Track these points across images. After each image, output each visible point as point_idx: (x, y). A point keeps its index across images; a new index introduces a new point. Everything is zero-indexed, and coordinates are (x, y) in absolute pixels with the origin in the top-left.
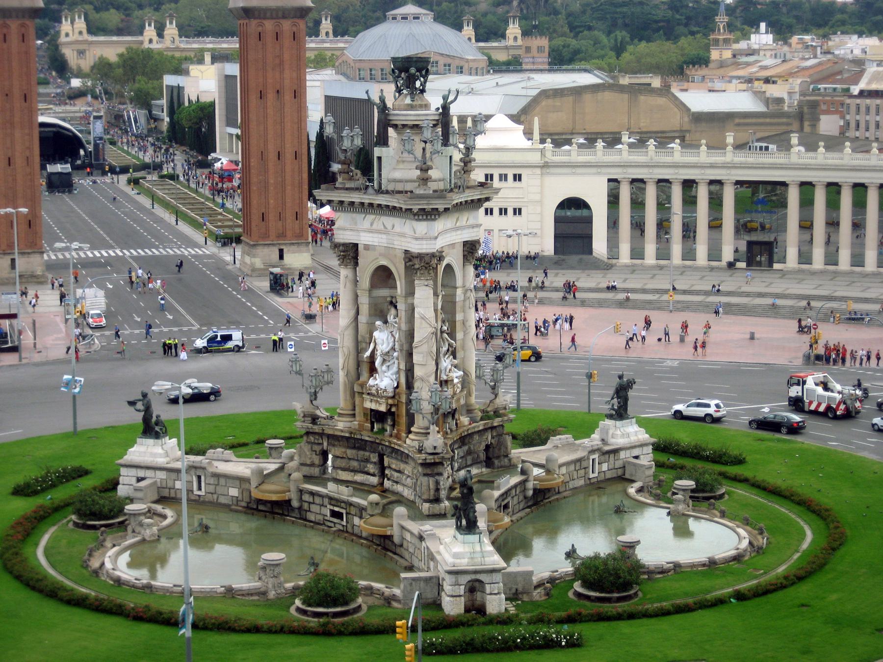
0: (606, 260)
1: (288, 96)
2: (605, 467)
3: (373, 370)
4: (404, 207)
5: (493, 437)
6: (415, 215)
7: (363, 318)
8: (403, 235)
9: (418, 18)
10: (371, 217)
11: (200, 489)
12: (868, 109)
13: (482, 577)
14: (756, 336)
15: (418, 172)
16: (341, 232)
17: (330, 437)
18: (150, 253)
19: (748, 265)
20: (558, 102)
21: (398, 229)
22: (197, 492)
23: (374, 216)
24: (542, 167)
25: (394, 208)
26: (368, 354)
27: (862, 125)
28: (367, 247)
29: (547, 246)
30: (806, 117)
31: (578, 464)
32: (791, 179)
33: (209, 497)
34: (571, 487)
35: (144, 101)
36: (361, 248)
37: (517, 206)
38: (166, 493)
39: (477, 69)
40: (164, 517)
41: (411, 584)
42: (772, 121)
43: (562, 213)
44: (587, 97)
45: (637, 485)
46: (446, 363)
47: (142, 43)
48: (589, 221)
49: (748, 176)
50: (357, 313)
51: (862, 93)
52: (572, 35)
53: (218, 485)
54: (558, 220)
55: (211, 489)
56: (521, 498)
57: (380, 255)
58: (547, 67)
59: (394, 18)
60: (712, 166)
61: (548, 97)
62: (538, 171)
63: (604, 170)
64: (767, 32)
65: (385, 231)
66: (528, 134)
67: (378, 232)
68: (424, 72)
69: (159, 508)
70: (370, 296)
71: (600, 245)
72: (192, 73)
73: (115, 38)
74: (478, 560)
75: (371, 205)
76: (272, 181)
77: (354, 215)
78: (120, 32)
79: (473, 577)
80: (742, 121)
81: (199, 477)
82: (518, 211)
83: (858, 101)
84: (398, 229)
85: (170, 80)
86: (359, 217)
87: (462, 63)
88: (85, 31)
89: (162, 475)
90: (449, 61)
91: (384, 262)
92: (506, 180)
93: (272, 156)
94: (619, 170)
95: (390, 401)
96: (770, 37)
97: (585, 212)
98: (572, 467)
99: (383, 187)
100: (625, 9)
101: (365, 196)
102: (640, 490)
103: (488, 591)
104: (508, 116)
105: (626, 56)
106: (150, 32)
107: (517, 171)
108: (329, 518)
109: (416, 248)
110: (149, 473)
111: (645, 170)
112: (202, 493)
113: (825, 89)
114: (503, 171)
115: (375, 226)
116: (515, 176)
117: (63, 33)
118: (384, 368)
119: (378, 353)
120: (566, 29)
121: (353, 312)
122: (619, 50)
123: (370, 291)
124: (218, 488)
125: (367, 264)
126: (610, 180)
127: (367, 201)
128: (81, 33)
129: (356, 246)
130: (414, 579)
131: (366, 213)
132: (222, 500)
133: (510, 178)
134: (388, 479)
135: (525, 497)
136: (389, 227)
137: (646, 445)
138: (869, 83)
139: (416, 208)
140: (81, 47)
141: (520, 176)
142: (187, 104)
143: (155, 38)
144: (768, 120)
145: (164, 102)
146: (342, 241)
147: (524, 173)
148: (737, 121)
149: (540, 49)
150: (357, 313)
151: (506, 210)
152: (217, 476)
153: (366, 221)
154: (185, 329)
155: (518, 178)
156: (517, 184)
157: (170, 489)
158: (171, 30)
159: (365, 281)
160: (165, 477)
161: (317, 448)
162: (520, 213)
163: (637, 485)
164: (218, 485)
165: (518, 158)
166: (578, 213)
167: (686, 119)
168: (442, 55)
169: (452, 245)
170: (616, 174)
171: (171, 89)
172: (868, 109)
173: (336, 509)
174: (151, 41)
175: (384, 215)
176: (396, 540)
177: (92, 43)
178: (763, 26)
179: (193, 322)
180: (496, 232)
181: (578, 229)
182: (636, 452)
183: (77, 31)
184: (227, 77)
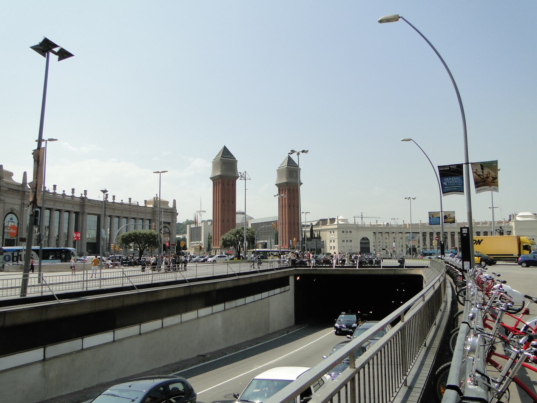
1: (296, 208)
29: (359, 250)
48: (369, 243)
54: (361, 243)
62: (356, 230)
76: (292, 231)
82: (351, 241)
93: (292, 224)
97: (367, 241)
133: (349, 232)
147: (352, 230)
155: (351, 232)
162: (351, 241)
166: (365, 241)
181: (367, 246)
184: (191, 228)
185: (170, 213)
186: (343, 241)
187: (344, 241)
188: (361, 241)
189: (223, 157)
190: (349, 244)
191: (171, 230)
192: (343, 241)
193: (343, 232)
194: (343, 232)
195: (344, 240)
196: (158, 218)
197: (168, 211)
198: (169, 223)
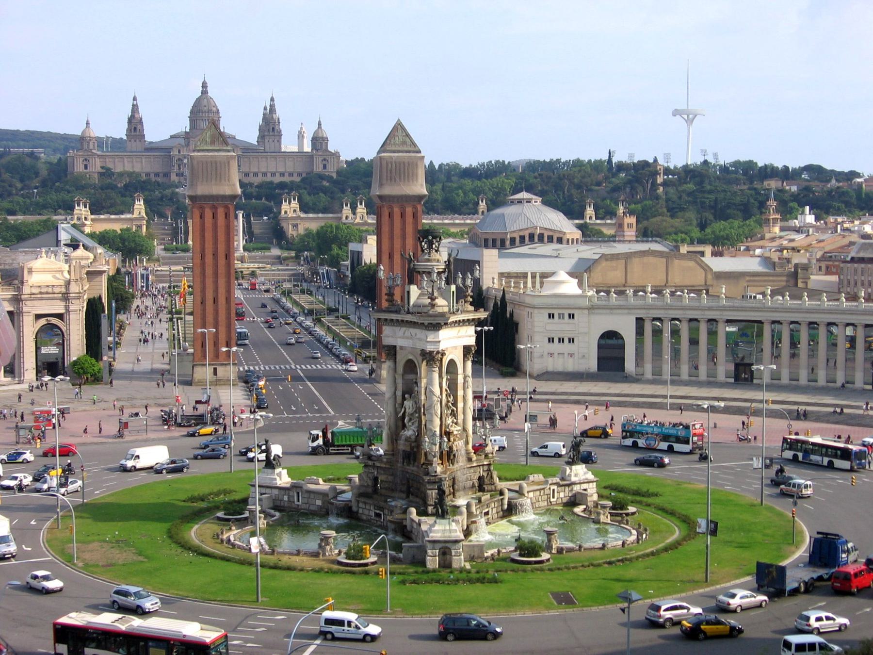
0: (635, 376)
2: (562, 495)
3: (404, 426)
4: (420, 322)
5: (483, 471)
6: (426, 327)
7: (399, 393)
8: (420, 340)
9: (530, 202)
10: (403, 329)
11: (298, 501)
12: (856, 270)
13: (448, 545)
14: (718, 426)
15: (429, 300)
16: (386, 338)
17: (378, 468)
18: (315, 368)
19: (735, 381)
20: (614, 263)
21: (418, 336)
22: (296, 503)
23: (405, 329)
24: (589, 309)
25: (415, 322)
26: (401, 414)
27: (852, 283)
28: (401, 348)
29: (592, 364)
30: (800, 276)
31: (542, 492)
32: (765, 318)
33: (304, 506)
34: (537, 506)
35: (334, 262)
36: (398, 349)
37: (571, 336)
38: (278, 503)
39: (573, 239)
40: (273, 516)
41: (408, 550)
42: (775, 278)
43: (603, 342)
44: (636, 261)
45: (583, 507)
46: (449, 421)
47: (341, 218)
48: (622, 347)
49: (734, 316)
50: (396, 389)
51: (853, 260)
52: (669, 214)
53: (309, 498)
54: (600, 347)
55: (306, 500)
56: (500, 509)
57: (409, 353)
58: (634, 239)
59: (512, 202)
60: (710, 309)
61: (607, 260)
62: (586, 312)
63: (633, 311)
64: (810, 214)
65: (411, 337)
66: (580, 285)
67: (407, 338)
68: (438, 239)
69: (272, 511)
70: (403, 379)
71: (630, 365)
72: (369, 242)
73: (320, 215)
74: (447, 534)
75: (402, 321)
77: (394, 328)
78: (325, 211)
79: (444, 545)
80: (752, 278)
81: (298, 493)
82: (571, 340)
83: (849, 265)
84: (418, 336)
85: (353, 246)
86: (397, 329)
87: (561, 236)
88: (298, 210)
89: (276, 492)
90: (551, 234)
91: (411, 357)
92: (563, 318)
94: (644, 311)
95: (413, 445)
96: (813, 217)
97: (620, 341)
98: (538, 493)
99: (411, 311)
100: (709, 196)
101: (399, 316)
102: (585, 510)
103: (453, 554)
104: (567, 273)
105: (708, 230)
106: (347, 210)
107: (571, 312)
108: (373, 517)
109: (429, 348)
110: (268, 491)
111: (662, 312)
112: (300, 503)
113: (835, 256)
114: (561, 311)
115: (406, 334)
116: (569, 315)
117: (283, 212)
118: (410, 424)
119: (407, 414)
120: (665, 210)
121: (393, 390)
122: (702, 226)
123: (403, 375)
124: (310, 500)
125: (401, 359)
126: (637, 319)
127: (400, 319)
128: (295, 211)
129: (395, 347)
130: (410, 547)
131: (401, 326)
132: (312, 508)
133: (566, 316)
134: (412, 495)
135: (502, 510)
136: (413, 334)
137: (592, 482)
138: (858, 252)
139: (426, 323)
140: (295, 222)
141: (573, 315)
142: (363, 264)
143: (351, 216)
144: (771, 278)
145: (348, 263)
146: (387, 344)
147: (576, 313)
148: (748, 278)
149: (630, 226)
150: (396, 389)
151: (563, 339)
152: (310, 492)
153: (401, 331)
154: (325, 415)
155: (571, 316)
156: (571, 321)
157: (281, 501)
158: (361, 209)
159: (400, 369)
160: (277, 493)
161: (371, 476)
162: (573, 341)
163: (583, 507)
164: (309, 498)
165: (572, 302)
167: (709, 277)
168: (546, 229)
169: (456, 348)
170: (641, 314)
171: (353, 252)
172: (856, 270)
173: (378, 512)
174: (347, 218)
175: (411, 327)
176: (409, 528)
177: (302, 219)
178: (807, 208)
179: (330, 410)
180: (556, 354)
182: (584, 486)
183: (292, 210)
185: (60, 295)
186: (551, 340)
187: (553, 341)
188: (603, 342)
189: (199, 151)
190: (566, 347)
191: (64, 329)
192: (551, 340)
193: (551, 316)
194: (551, 316)
195: (553, 339)
196: (25, 309)
197: (57, 290)
198: (60, 316)
